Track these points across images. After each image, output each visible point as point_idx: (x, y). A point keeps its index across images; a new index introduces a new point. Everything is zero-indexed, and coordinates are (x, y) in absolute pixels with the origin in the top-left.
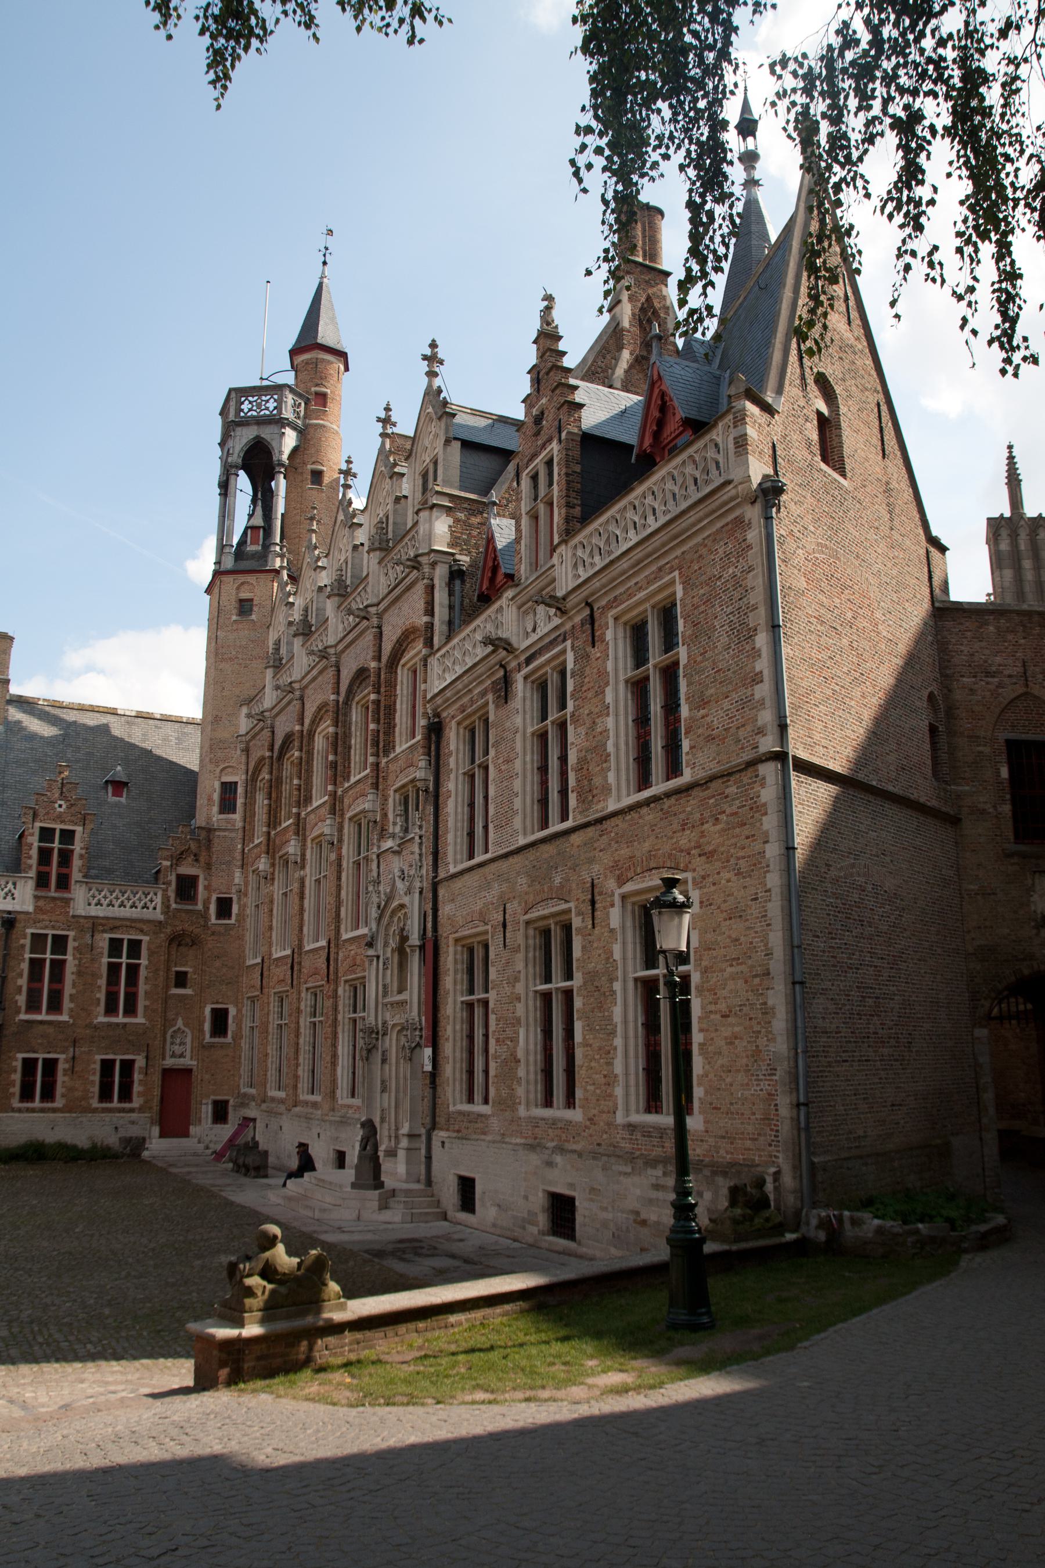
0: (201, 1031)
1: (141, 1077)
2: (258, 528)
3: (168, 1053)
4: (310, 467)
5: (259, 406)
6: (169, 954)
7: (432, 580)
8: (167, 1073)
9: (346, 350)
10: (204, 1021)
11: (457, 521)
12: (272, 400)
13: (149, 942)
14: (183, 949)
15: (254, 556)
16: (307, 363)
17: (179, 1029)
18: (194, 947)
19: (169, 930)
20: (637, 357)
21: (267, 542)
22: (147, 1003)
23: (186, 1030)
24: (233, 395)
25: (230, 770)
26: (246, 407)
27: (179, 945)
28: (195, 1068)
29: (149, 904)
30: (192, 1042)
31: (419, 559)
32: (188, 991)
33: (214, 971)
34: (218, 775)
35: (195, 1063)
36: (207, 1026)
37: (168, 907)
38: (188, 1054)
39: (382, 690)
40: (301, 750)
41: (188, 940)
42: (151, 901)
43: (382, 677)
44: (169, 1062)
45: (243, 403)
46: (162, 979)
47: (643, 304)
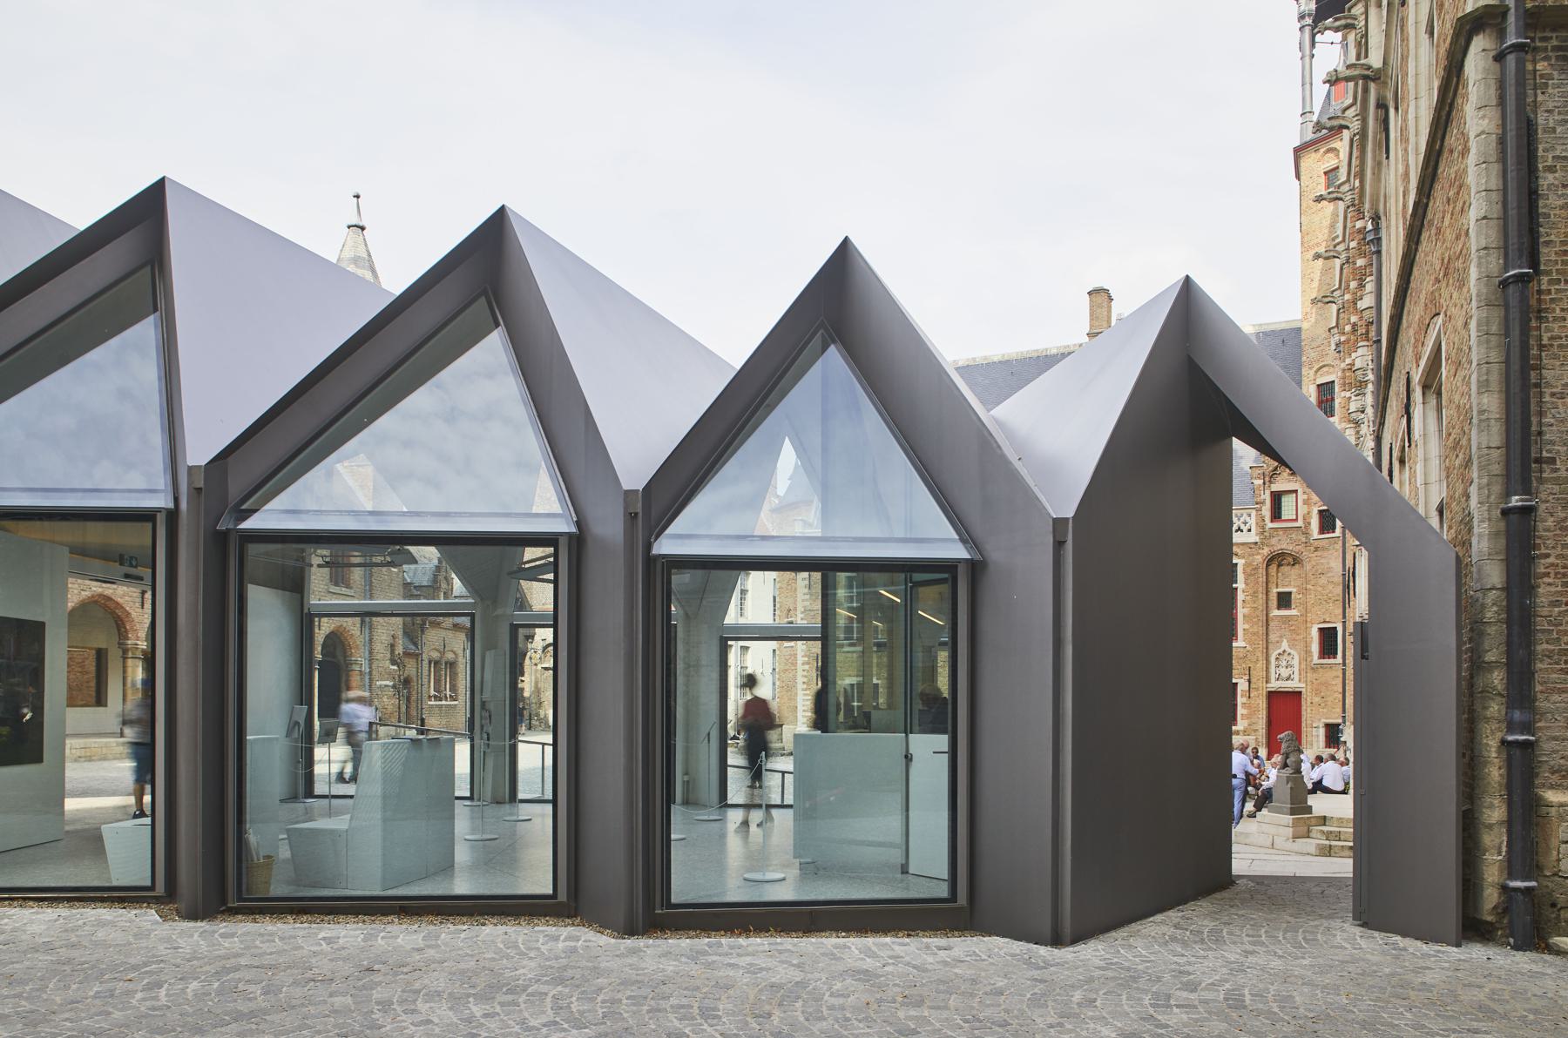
0: (1308, 652)
1: (1244, 700)
3: (1273, 676)
6: (1267, 575)
8: (1272, 696)
10: (1311, 642)
13: (1244, 565)
14: (1285, 569)
17: (1284, 651)
18: (1297, 566)
19: (1266, 551)
22: (1246, 626)
23: (1292, 652)
25: (1325, 369)
27: (1279, 565)
28: (1303, 690)
29: (1242, 527)
30: (1300, 663)
32: (1293, 612)
33: (1320, 589)
34: (1312, 378)
35: (1304, 685)
36: (1315, 648)
37: (1263, 528)
38: (1296, 676)
41: (1291, 560)
42: (1245, 523)
44: (1274, 685)
46: (1261, 601)
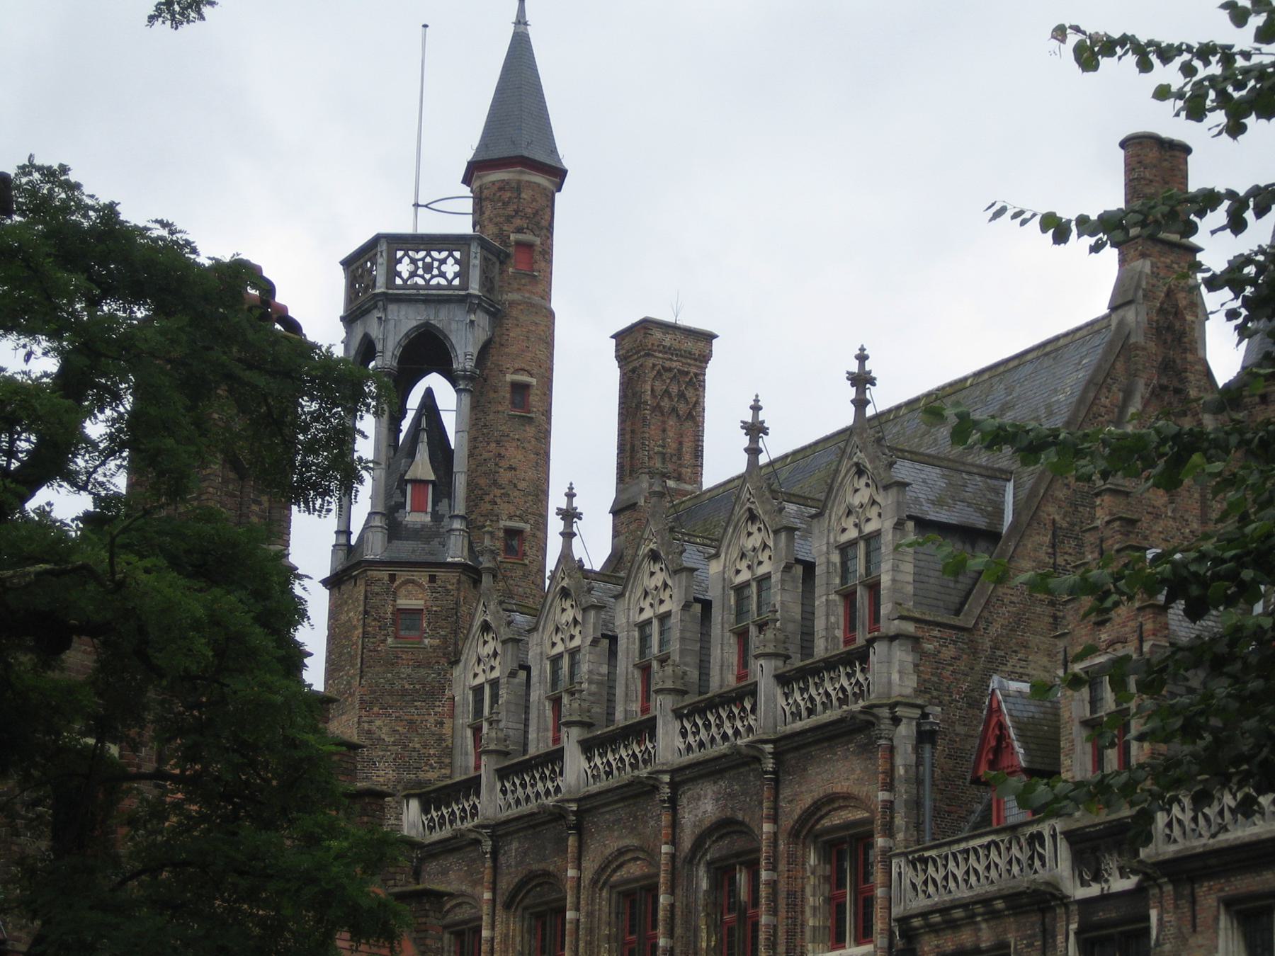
2: (426, 482)
4: (509, 377)
5: (428, 268)
7: (891, 740)
9: (566, 163)
11: (923, 654)
12: (451, 261)
15: (417, 534)
16: (503, 186)
20: (1154, 388)
21: (443, 507)
24: (383, 247)
26: (404, 268)
31: (875, 711)
39: (782, 866)
40: (578, 909)
43: (782, 847)
45: (400, 261)
47: (1162, 303)
